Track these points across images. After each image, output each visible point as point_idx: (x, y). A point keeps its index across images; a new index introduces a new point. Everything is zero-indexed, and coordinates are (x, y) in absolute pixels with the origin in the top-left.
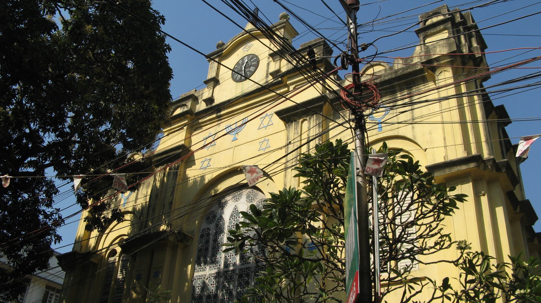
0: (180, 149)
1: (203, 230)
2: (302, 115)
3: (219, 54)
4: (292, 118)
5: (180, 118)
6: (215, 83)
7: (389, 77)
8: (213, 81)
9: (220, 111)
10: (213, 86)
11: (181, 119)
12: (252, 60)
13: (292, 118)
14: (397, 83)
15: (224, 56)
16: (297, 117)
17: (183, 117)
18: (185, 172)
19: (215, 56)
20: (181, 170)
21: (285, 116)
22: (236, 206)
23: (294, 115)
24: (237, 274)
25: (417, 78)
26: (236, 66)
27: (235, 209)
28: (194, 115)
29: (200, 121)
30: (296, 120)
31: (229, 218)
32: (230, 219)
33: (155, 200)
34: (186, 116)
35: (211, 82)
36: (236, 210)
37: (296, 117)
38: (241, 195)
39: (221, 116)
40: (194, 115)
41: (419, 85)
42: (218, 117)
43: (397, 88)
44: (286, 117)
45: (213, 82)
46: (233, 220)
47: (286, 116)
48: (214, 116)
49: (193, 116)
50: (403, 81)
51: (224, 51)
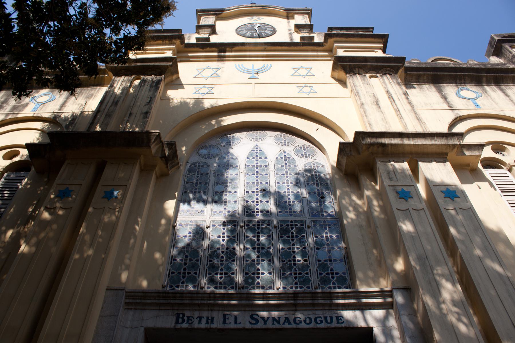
0: (170, 62)
1: (193, 164)
2: (370, 71)
3: (217, 12)
4: (357, 69)
5: (163, 41)
6: (212, 32)
7: (478, 66)
8: (212, 28)
9: (225, 52)
10: (209, 32)
11: (164, 42)
12: (266, 27)
13: (357, 69)
14: (485, 74)
15: (222, 18)
16: (363, 70)
17: (169, 40)
18: (165, 92)
19: (212, 13)
20: (162, 86)
21: (347, 65)
22: (257, 145)
23: (360, 67)
24: (275, 227)
25: (509, 76)
26: (242, 27)
27: (257, 148)
28: (183, 45)
29: (190, 55)
30: (360, 73)
31: (246, 156)
32: (248, 158)
33: (111, 106)
34: (174, 41)
35: (209, 28)
36: (259, 149)
37: (362, 70)
38: (264, 138)
39: (224, 57)
40: (183, 45)
41: (508, 84)
42: (219, 57)
43: (484, 79)
44: (348, 66)
45: (209, 30)
46: (255, 160)
47: (350, 65)
48: (215, 54)
49: (182, 46)
50: (492, 75)
51: (224, 12)
